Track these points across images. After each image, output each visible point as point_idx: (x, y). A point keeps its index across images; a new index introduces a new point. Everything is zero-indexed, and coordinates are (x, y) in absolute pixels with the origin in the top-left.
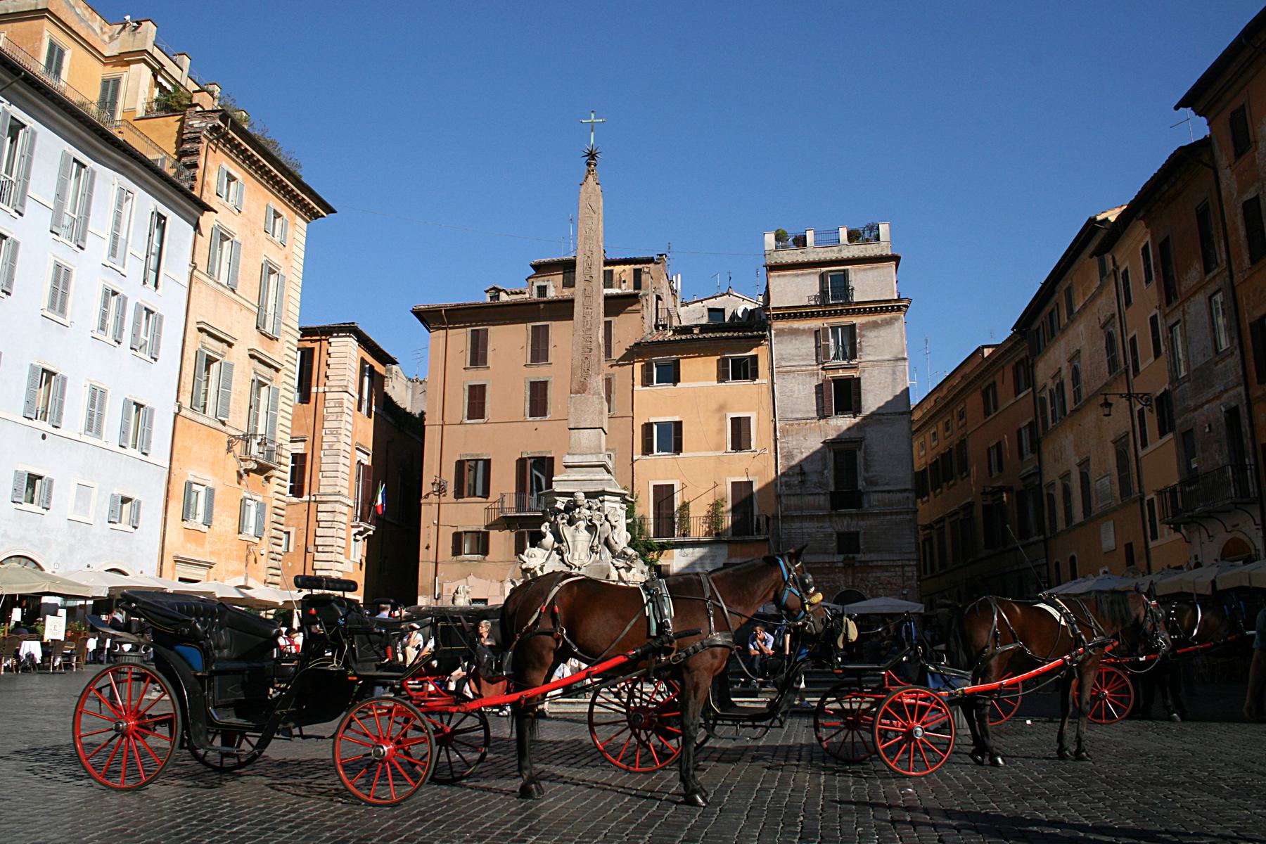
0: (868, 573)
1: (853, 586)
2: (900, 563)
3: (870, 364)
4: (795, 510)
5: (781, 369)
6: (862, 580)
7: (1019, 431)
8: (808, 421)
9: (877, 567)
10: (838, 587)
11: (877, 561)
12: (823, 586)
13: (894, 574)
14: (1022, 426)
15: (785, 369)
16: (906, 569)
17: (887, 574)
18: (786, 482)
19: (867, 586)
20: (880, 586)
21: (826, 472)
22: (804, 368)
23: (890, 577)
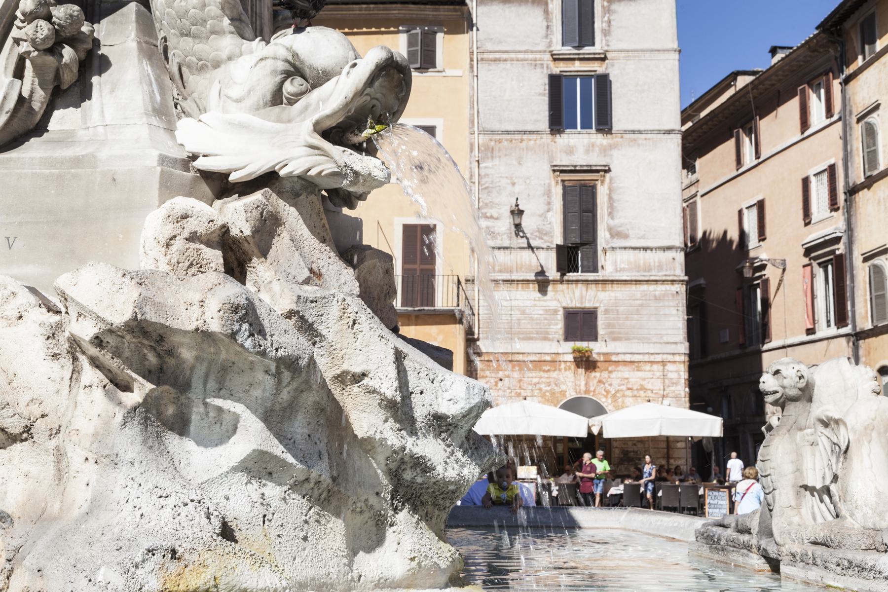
0: (610, 372)
1: (587, 391)
2: (659, 358)
3: (623, 54)
4: (500, 271)
5: (486, 56)
6: (600, 381)
7: (806, 182)
8: (525, 137)
9: (625, 362)
10: (563, 393)
11: (624, 353)
12: (540, 389)
13: (649, 375)
14: (811, 172)
15: (492, 56)
16: (670, 367)
17: (640, 374)
18: (488, 228)
19: (608, 392)
20: (629, 393)
21: (549, 214)
22: (521, 56)
23: (644, 379)
